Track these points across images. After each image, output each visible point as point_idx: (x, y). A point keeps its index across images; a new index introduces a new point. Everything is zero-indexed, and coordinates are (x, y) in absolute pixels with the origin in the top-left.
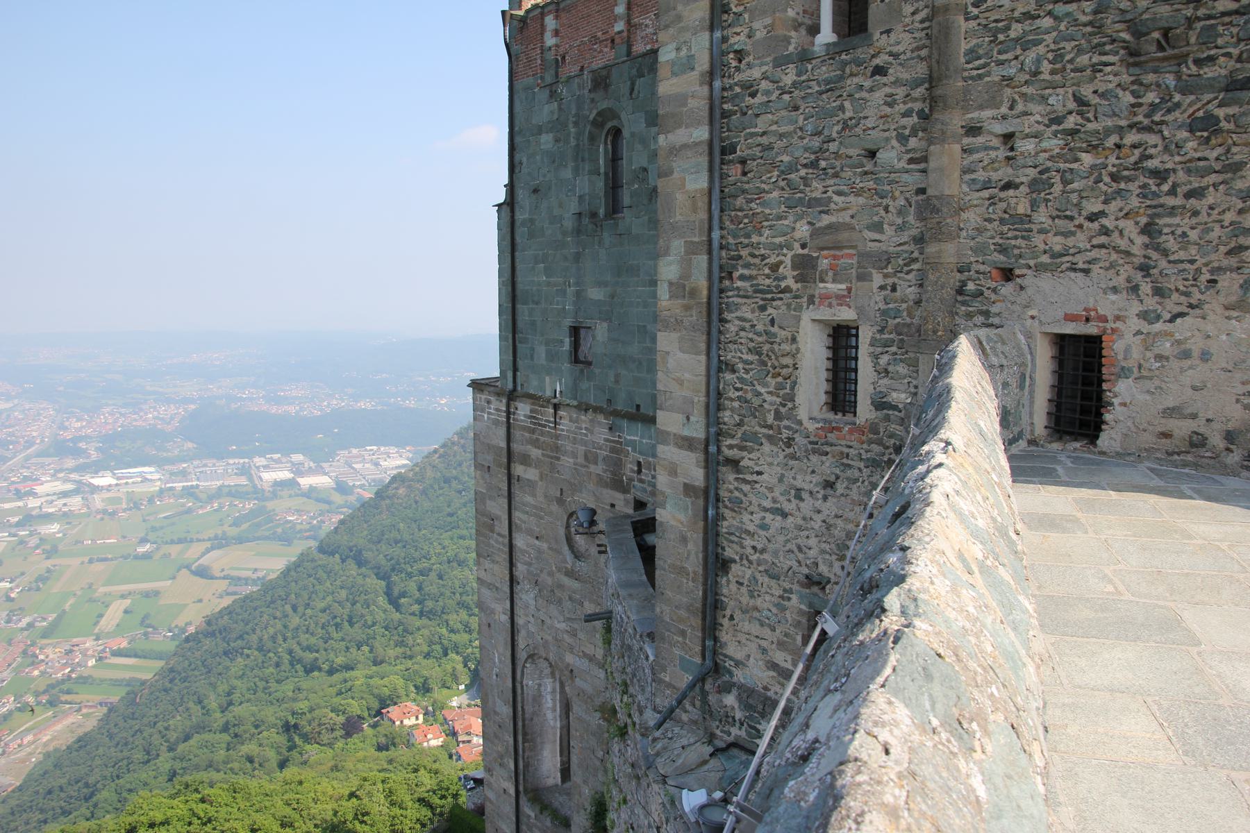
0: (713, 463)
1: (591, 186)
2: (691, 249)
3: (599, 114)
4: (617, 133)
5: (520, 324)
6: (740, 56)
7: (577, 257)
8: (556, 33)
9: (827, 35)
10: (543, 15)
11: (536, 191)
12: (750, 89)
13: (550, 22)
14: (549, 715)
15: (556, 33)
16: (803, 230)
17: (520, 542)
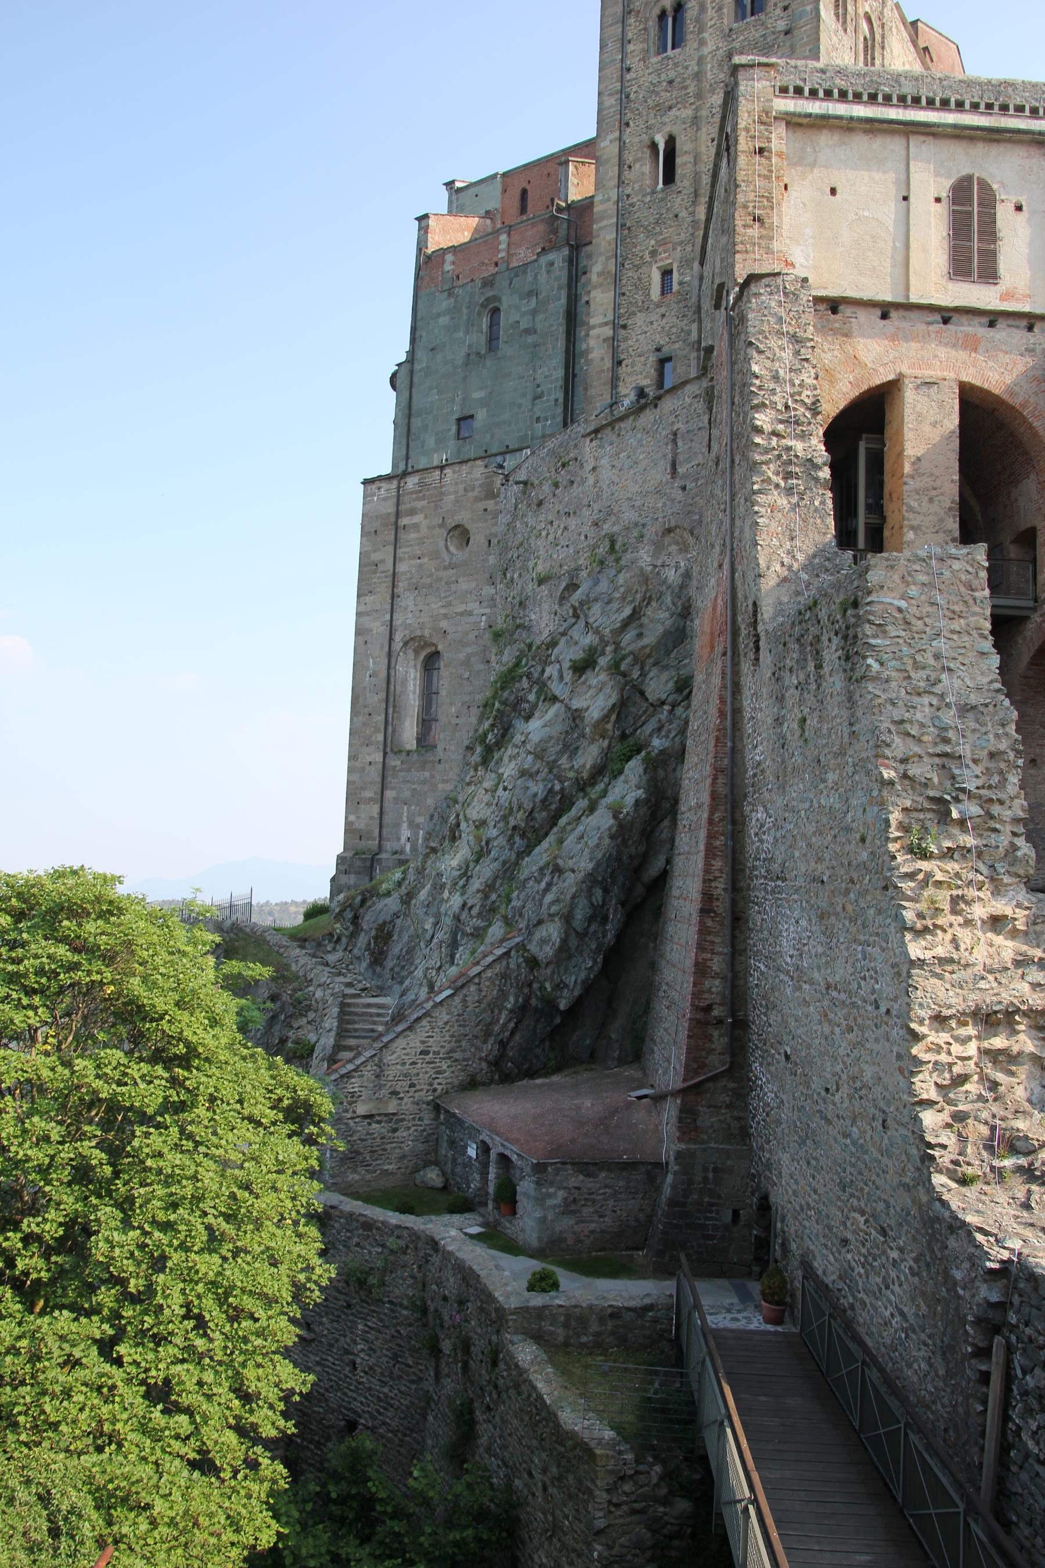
0: (619, 325)
1: (478, 339)
2: (608, 258)
3: (487, 300)
4: (496, 311)
5: (413, 429)
6: (628, 196)
7: (465, 379)
8: (453, 263)
9: (661, 185)
10: (444, 254)
11: (433, 350)
12: (632, 205)
13: (449, 258)
14: (411, 696)
15: (453, 263)
16: (653, 242)
17: (402, 568)
